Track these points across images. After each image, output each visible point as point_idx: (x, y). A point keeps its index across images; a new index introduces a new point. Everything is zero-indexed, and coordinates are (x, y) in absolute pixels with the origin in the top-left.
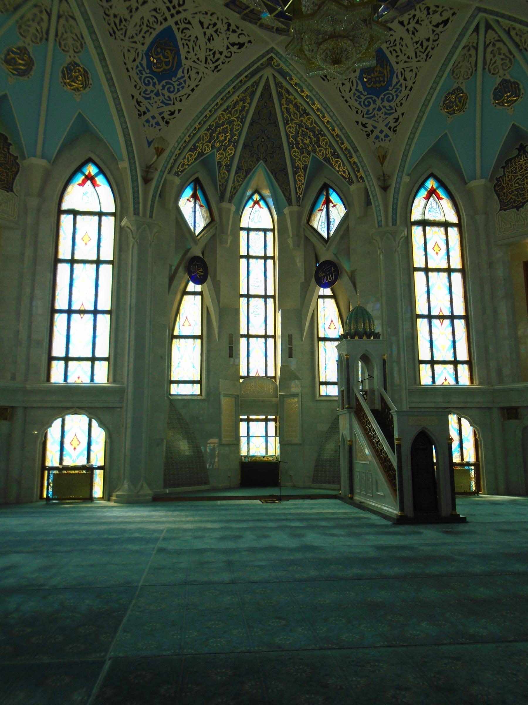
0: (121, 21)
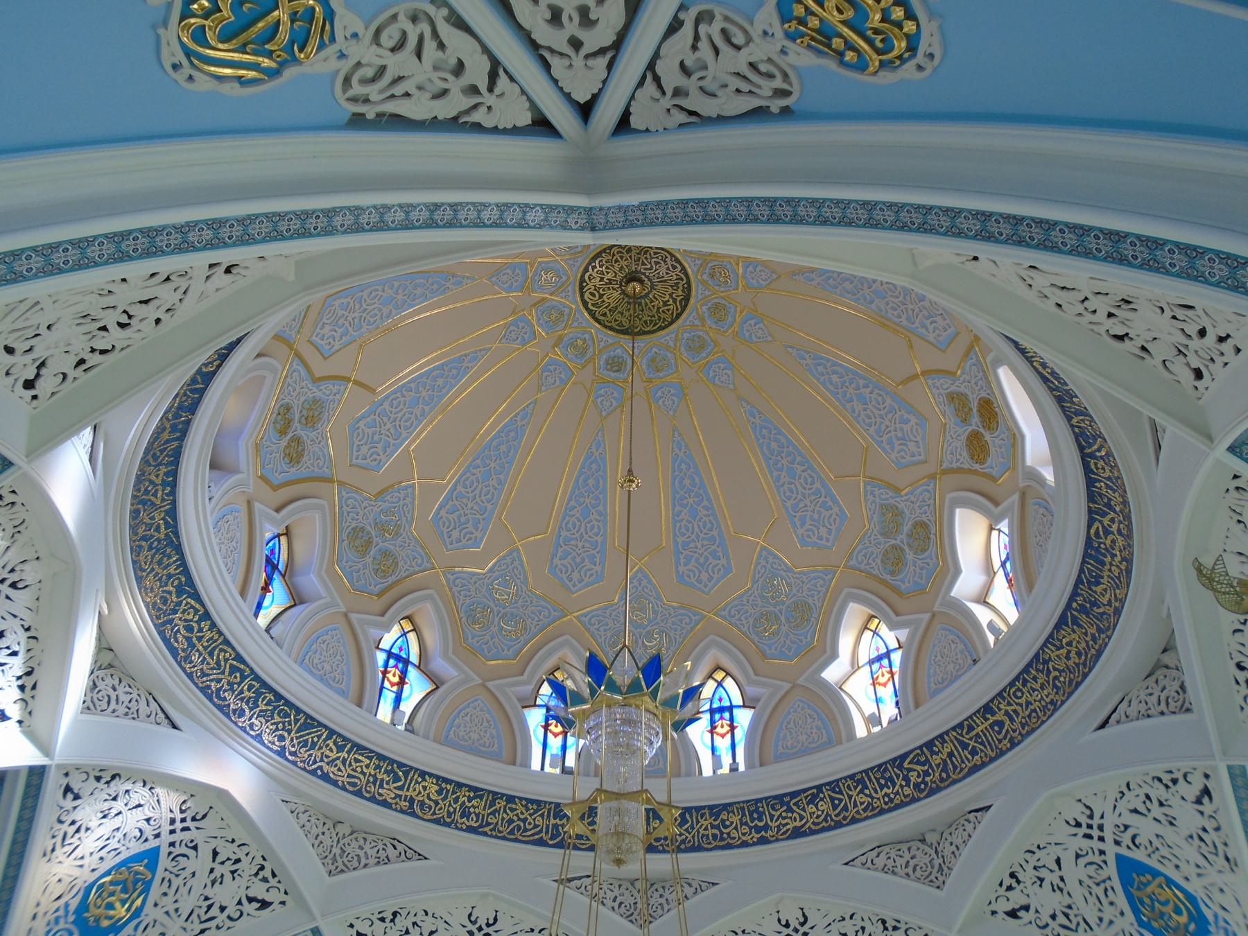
0: (1067, 916)
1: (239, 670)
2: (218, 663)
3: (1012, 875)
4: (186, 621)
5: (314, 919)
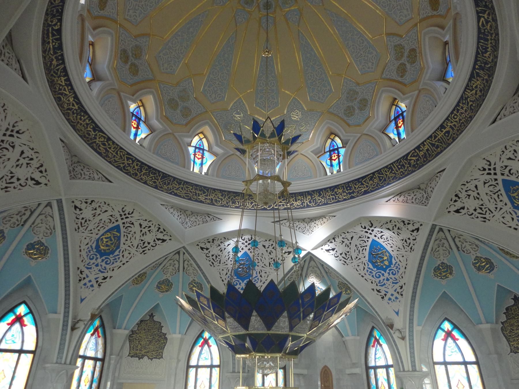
0: (481, 209)
1: (130, 158)
2: (121, 156)
3: (456, 196)
4: (101, 141)
5: (182, 243)
